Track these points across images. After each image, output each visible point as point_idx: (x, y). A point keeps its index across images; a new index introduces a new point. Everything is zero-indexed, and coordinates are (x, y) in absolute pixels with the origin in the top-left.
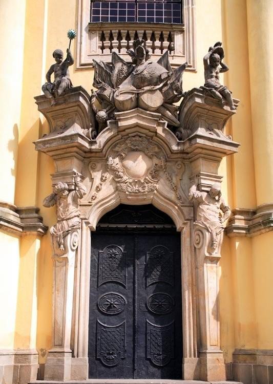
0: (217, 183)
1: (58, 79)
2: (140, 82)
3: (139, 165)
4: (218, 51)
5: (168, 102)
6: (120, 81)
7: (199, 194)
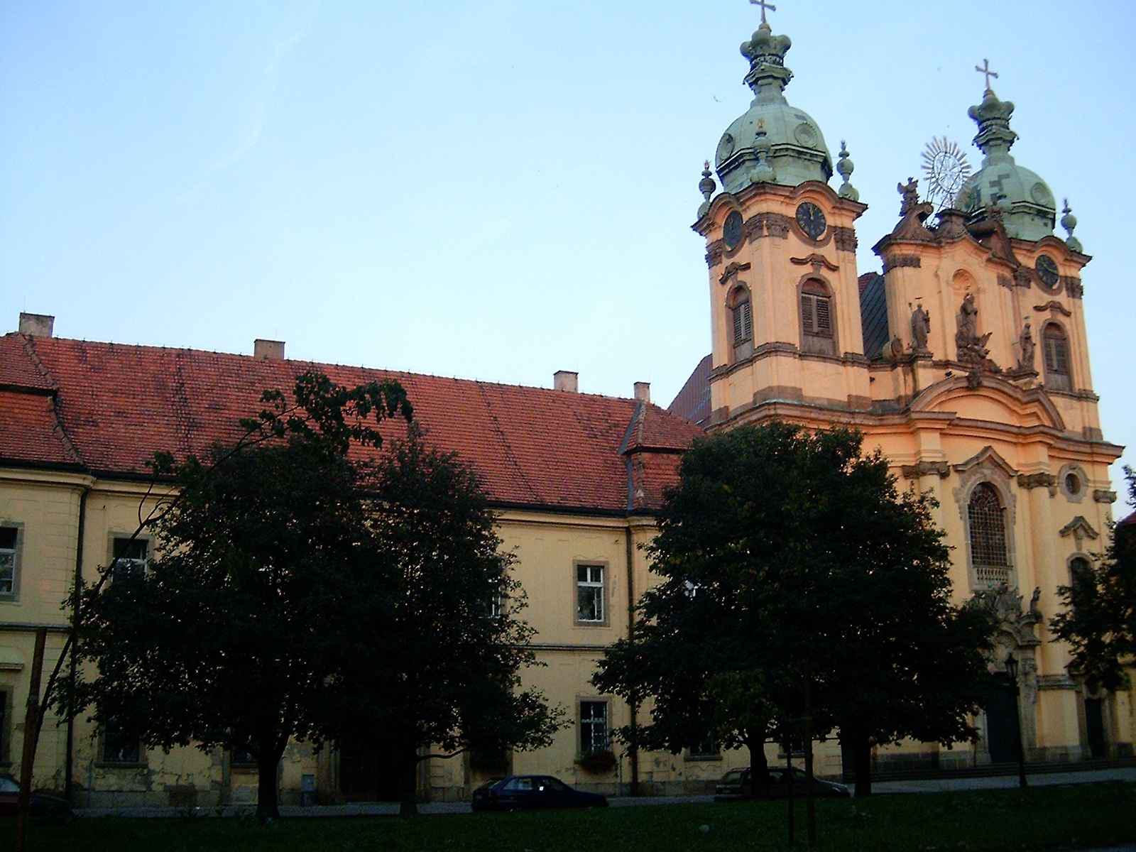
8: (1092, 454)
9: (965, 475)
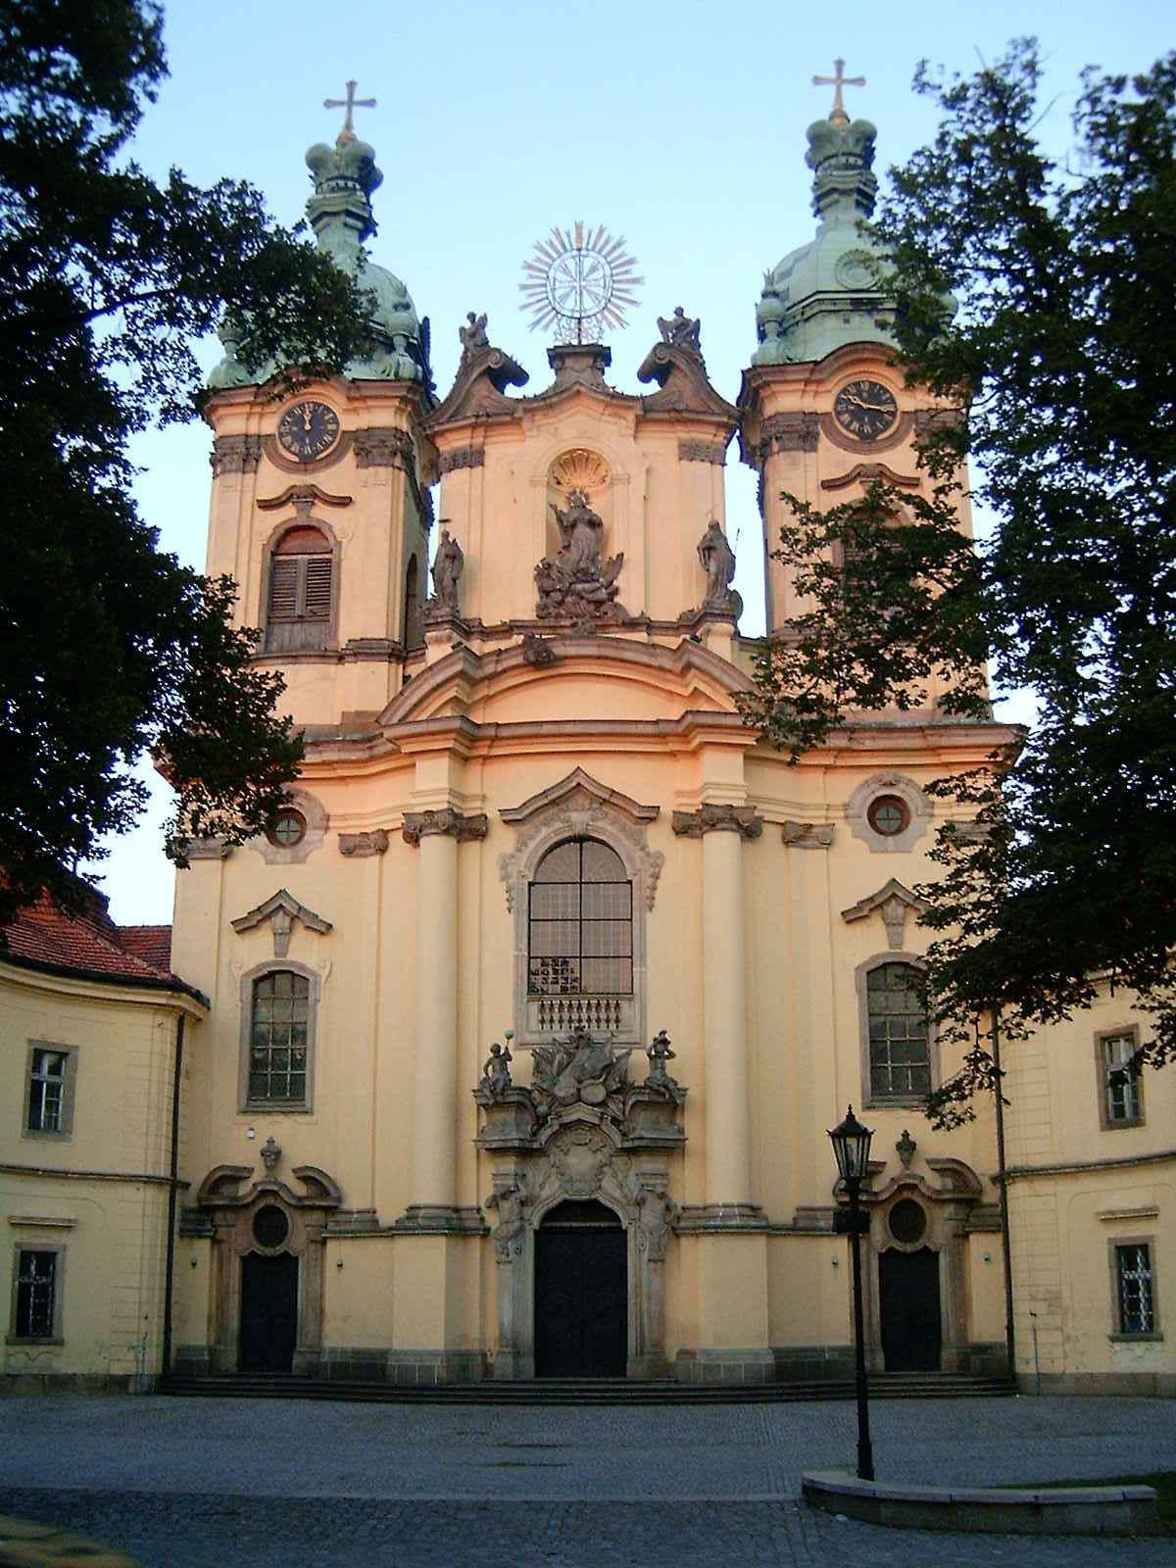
1: (497, 1076)
8: (934, 750)
9: (525, 828)
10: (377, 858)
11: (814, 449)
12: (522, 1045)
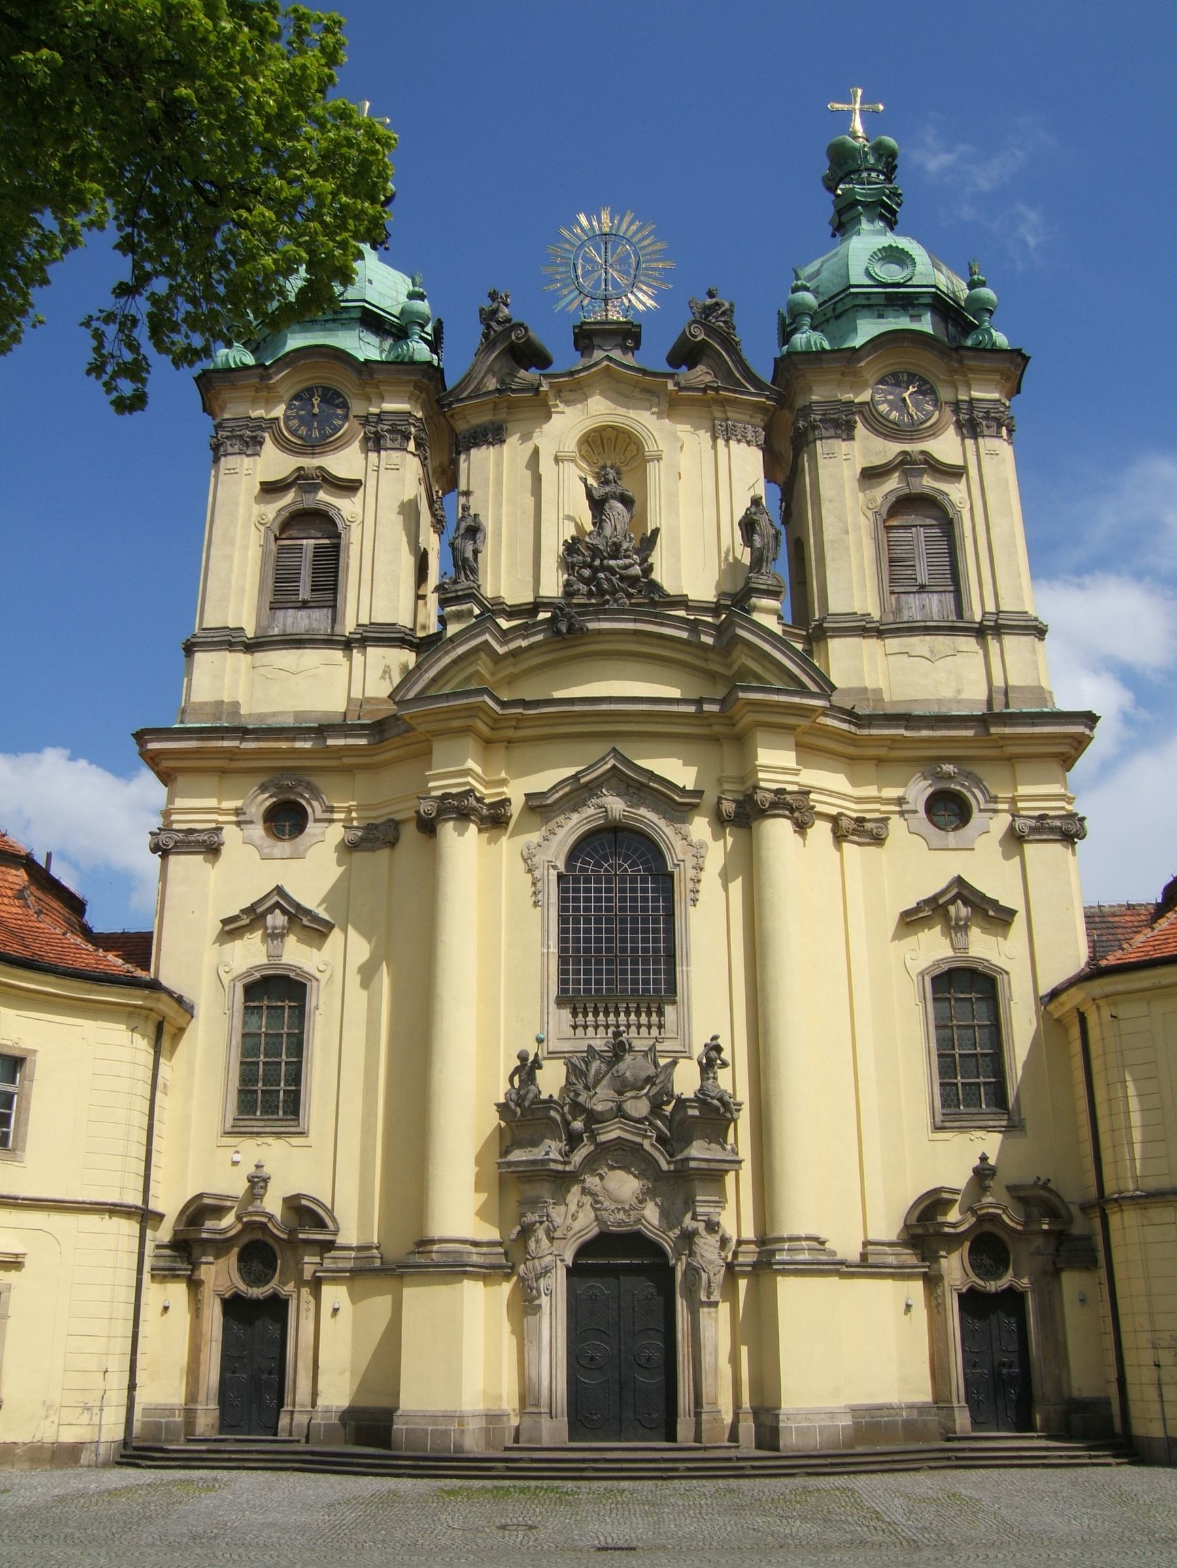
0: (718, 1210)
2: (623, 1087)
3: (624, 1185)
4: (714, 1048)
5: (656, 1107)
6: (597, 1082)
7: (694, 1224)
10: (385, 853)
11: (853, 439)
12: (553, 1055)
